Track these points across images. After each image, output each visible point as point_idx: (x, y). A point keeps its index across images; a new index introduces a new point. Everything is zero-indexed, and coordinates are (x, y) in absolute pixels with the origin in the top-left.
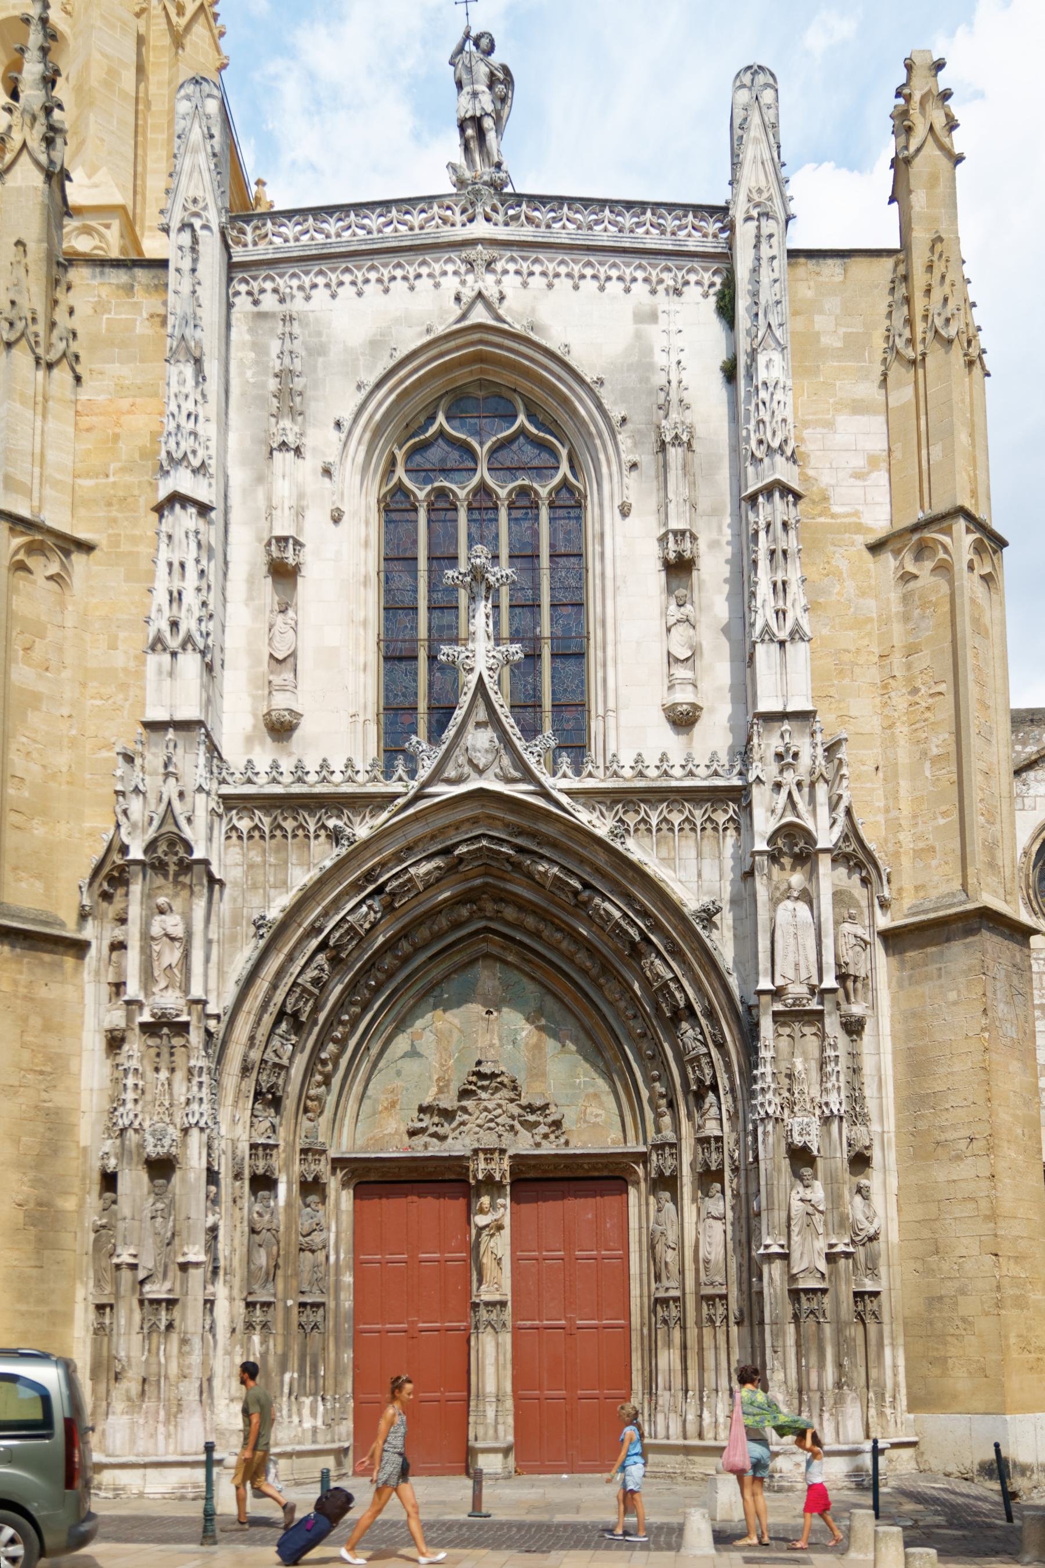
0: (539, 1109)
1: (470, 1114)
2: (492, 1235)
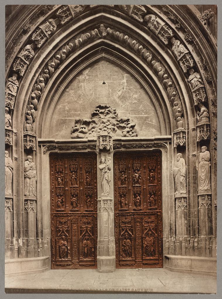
0: (125, 121)
1: (96, 124)
2: (106, 172)
